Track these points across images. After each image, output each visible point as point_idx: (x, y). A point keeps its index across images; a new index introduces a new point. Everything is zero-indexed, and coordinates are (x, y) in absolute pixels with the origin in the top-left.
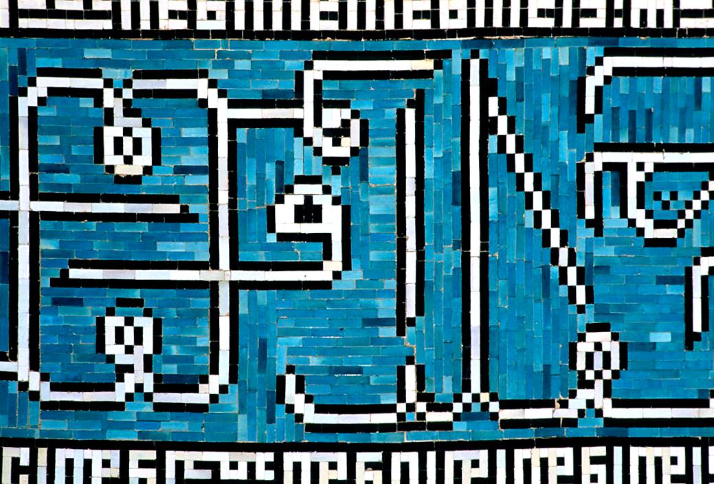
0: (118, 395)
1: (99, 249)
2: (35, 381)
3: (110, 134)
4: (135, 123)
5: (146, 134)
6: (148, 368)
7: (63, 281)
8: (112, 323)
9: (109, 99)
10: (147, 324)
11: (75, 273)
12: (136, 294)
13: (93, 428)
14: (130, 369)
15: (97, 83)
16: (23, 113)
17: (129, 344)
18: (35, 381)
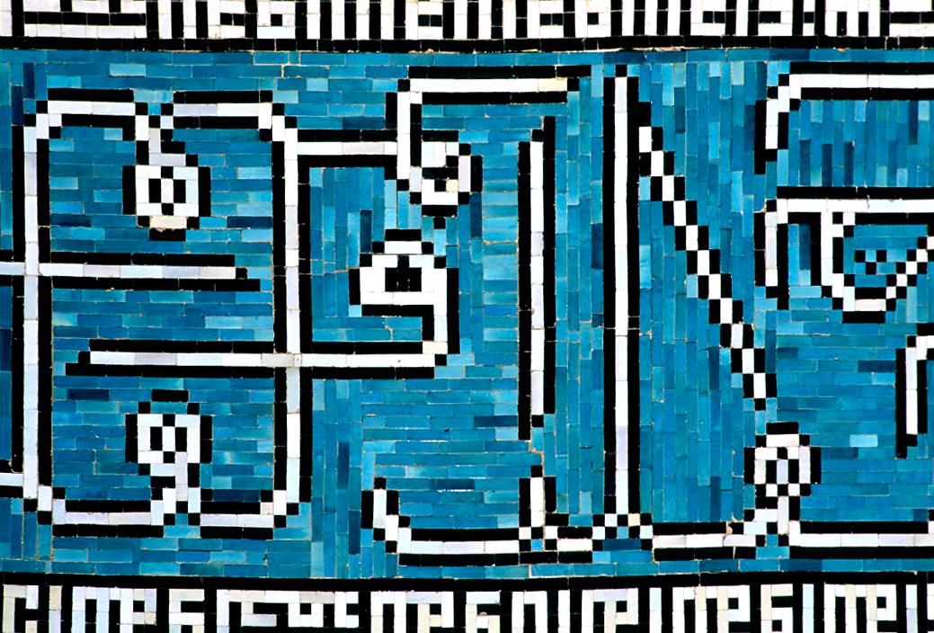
0: (154, 517)
1: (129, 326)
2: (45, 499)
3: (143, 175)
4: (177, 160)
5: (190, 176)
6: (193, 482)
7: (82, 367)
8: (146, 422)
9: (143, 130)
10: (192, 424)
11: (98, 358)
12: (178, 384)
13: (121, 560)
14: (170, 482)
15: (127, 109)
16: (30, 147)
17: (169, 450)
18: (45, 499)
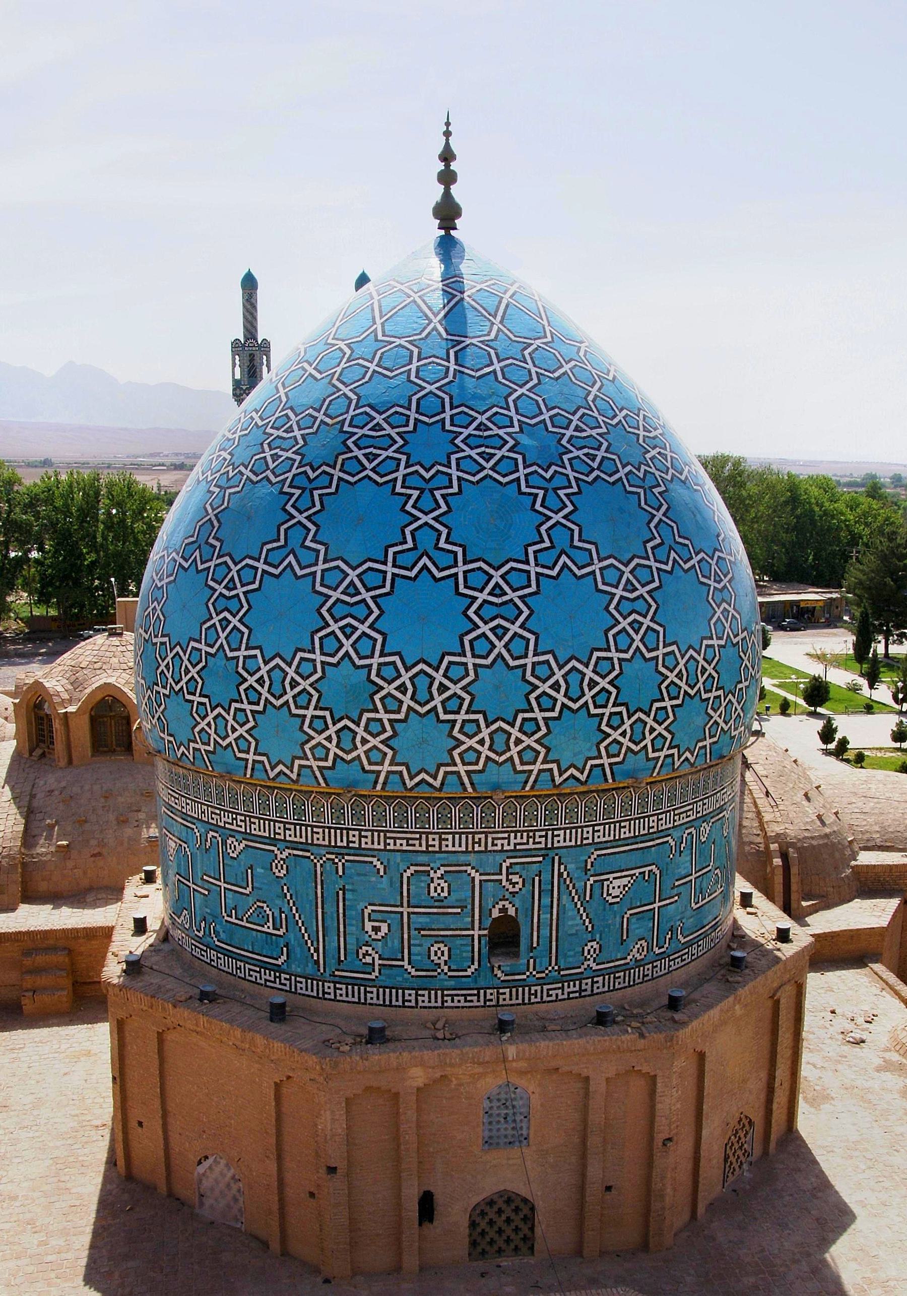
16: (476, 963)
